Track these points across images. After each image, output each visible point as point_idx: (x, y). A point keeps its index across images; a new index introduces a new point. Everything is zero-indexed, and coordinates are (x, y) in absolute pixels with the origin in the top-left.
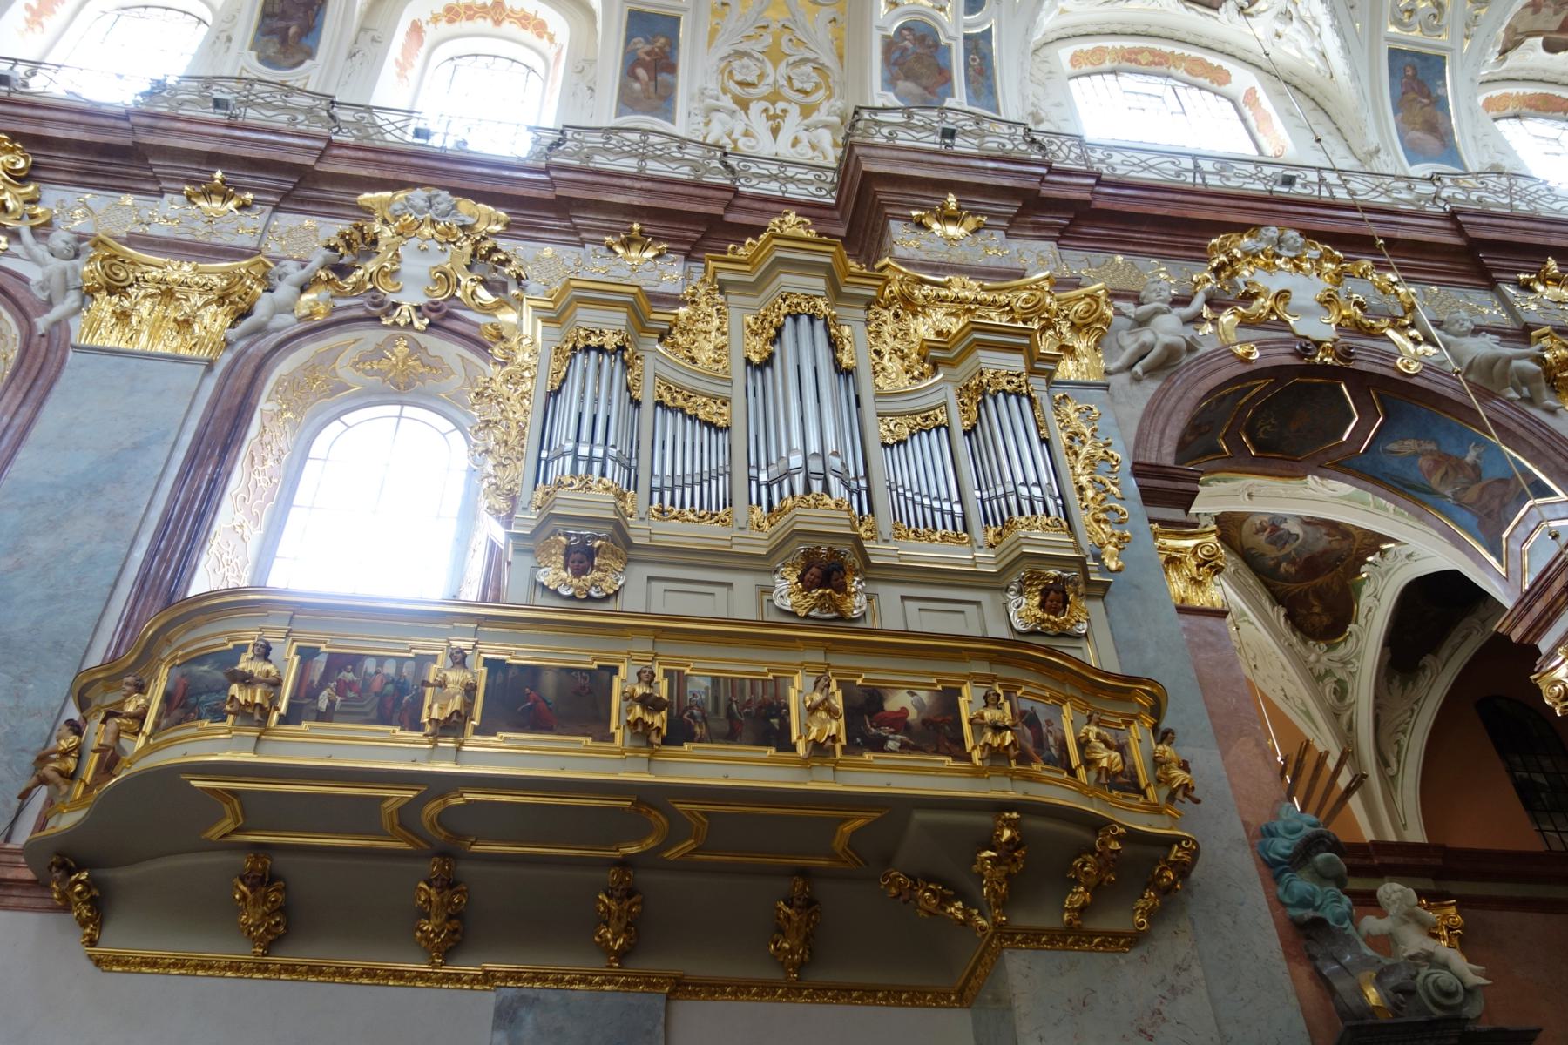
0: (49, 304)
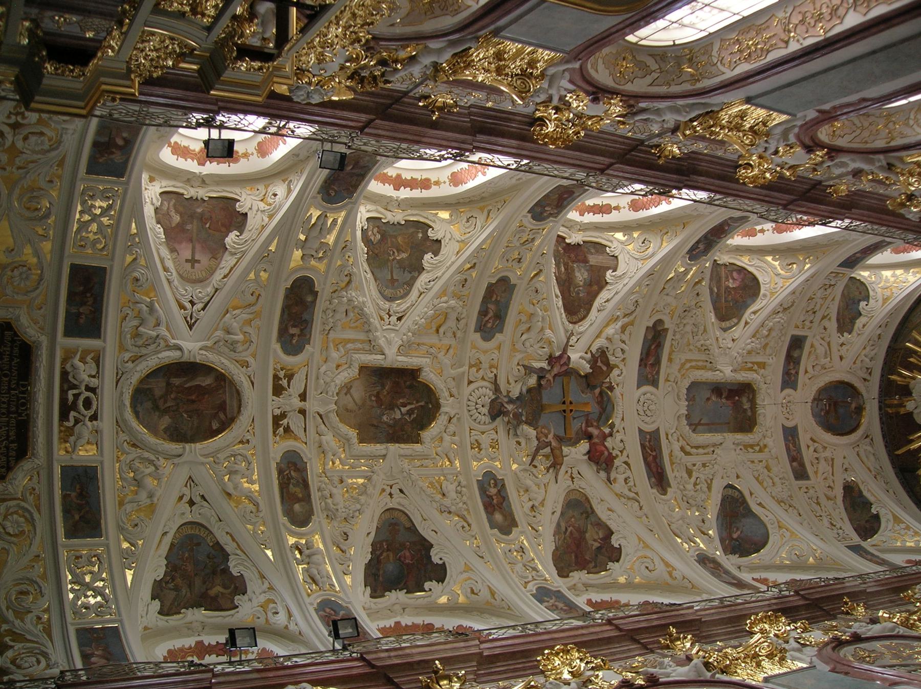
0: (564, 71)
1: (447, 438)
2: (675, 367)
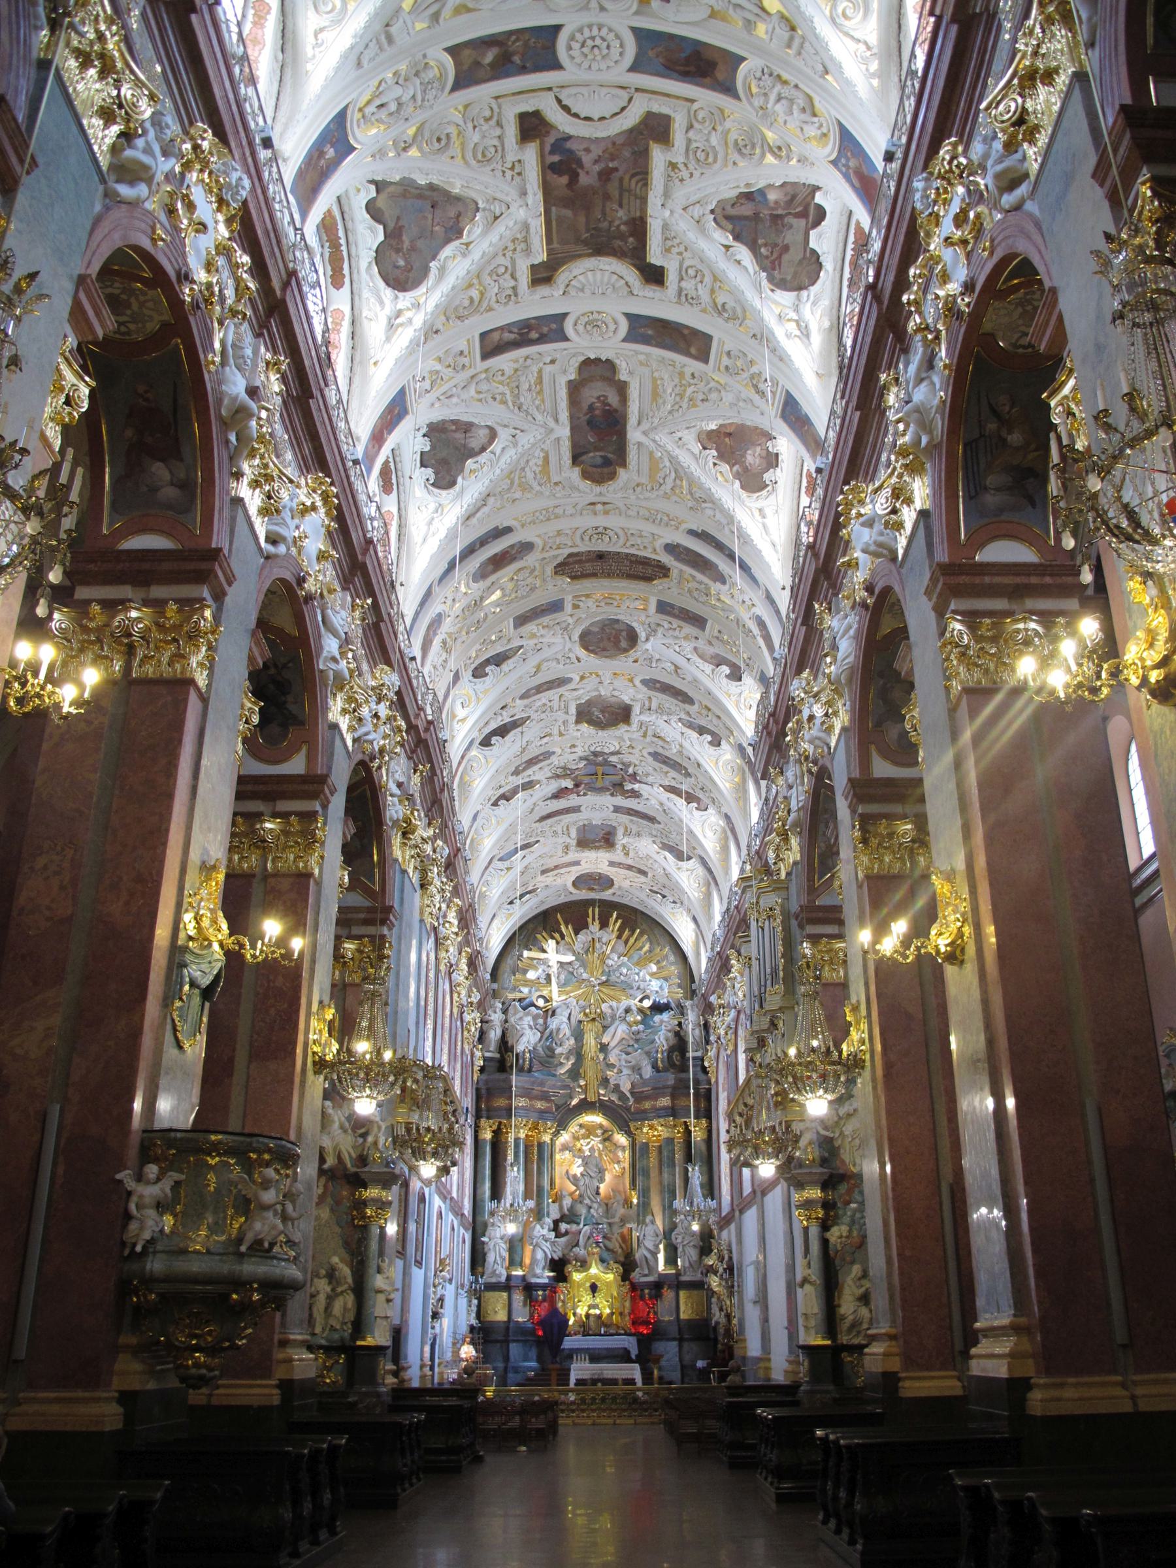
1: (579, 734)
2: (627, 822)
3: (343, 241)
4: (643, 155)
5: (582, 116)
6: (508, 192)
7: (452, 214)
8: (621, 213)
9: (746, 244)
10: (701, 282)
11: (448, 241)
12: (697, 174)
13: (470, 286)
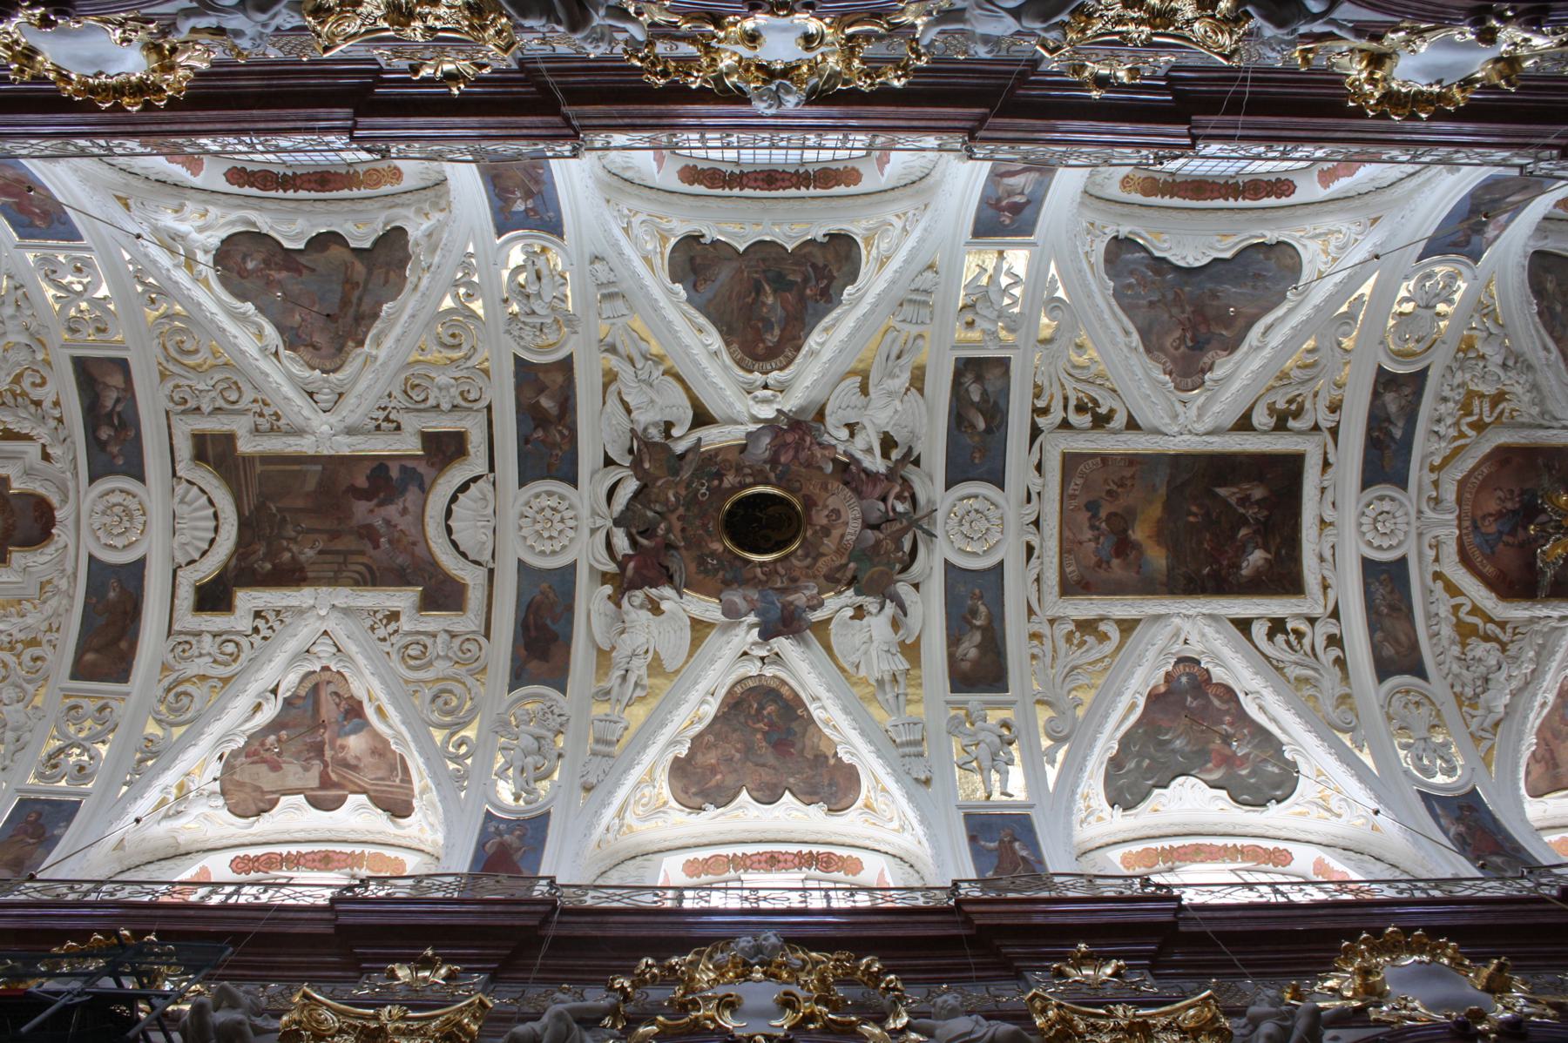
3: (290, 194)
4: (400, 578)
5: (453, 507)
6: (355, 409)
7: (317, 338)
8: (309, 553)
9: (278, 716)
10: (215, 661)
11: (281, 329)
12: (386, 647)
13: (214, 353)
